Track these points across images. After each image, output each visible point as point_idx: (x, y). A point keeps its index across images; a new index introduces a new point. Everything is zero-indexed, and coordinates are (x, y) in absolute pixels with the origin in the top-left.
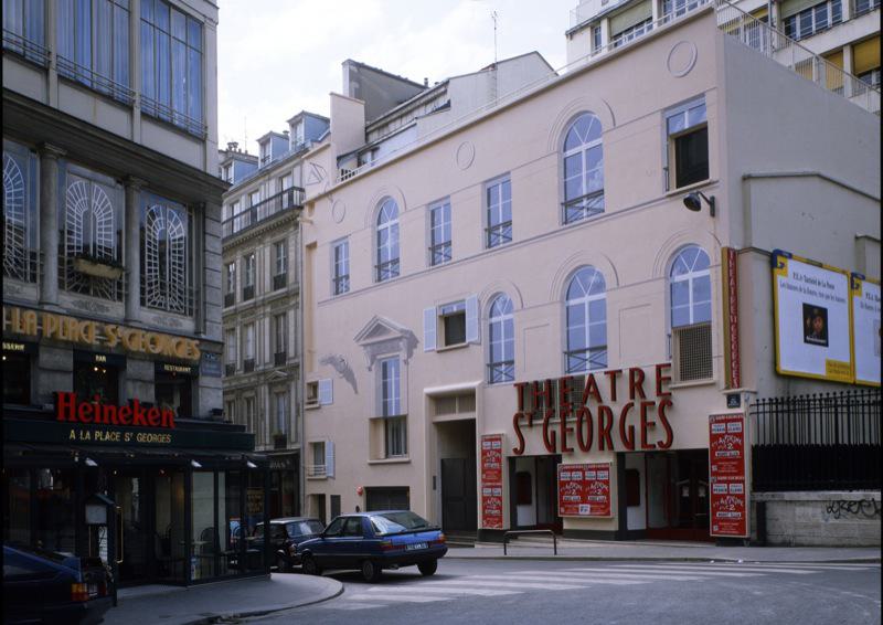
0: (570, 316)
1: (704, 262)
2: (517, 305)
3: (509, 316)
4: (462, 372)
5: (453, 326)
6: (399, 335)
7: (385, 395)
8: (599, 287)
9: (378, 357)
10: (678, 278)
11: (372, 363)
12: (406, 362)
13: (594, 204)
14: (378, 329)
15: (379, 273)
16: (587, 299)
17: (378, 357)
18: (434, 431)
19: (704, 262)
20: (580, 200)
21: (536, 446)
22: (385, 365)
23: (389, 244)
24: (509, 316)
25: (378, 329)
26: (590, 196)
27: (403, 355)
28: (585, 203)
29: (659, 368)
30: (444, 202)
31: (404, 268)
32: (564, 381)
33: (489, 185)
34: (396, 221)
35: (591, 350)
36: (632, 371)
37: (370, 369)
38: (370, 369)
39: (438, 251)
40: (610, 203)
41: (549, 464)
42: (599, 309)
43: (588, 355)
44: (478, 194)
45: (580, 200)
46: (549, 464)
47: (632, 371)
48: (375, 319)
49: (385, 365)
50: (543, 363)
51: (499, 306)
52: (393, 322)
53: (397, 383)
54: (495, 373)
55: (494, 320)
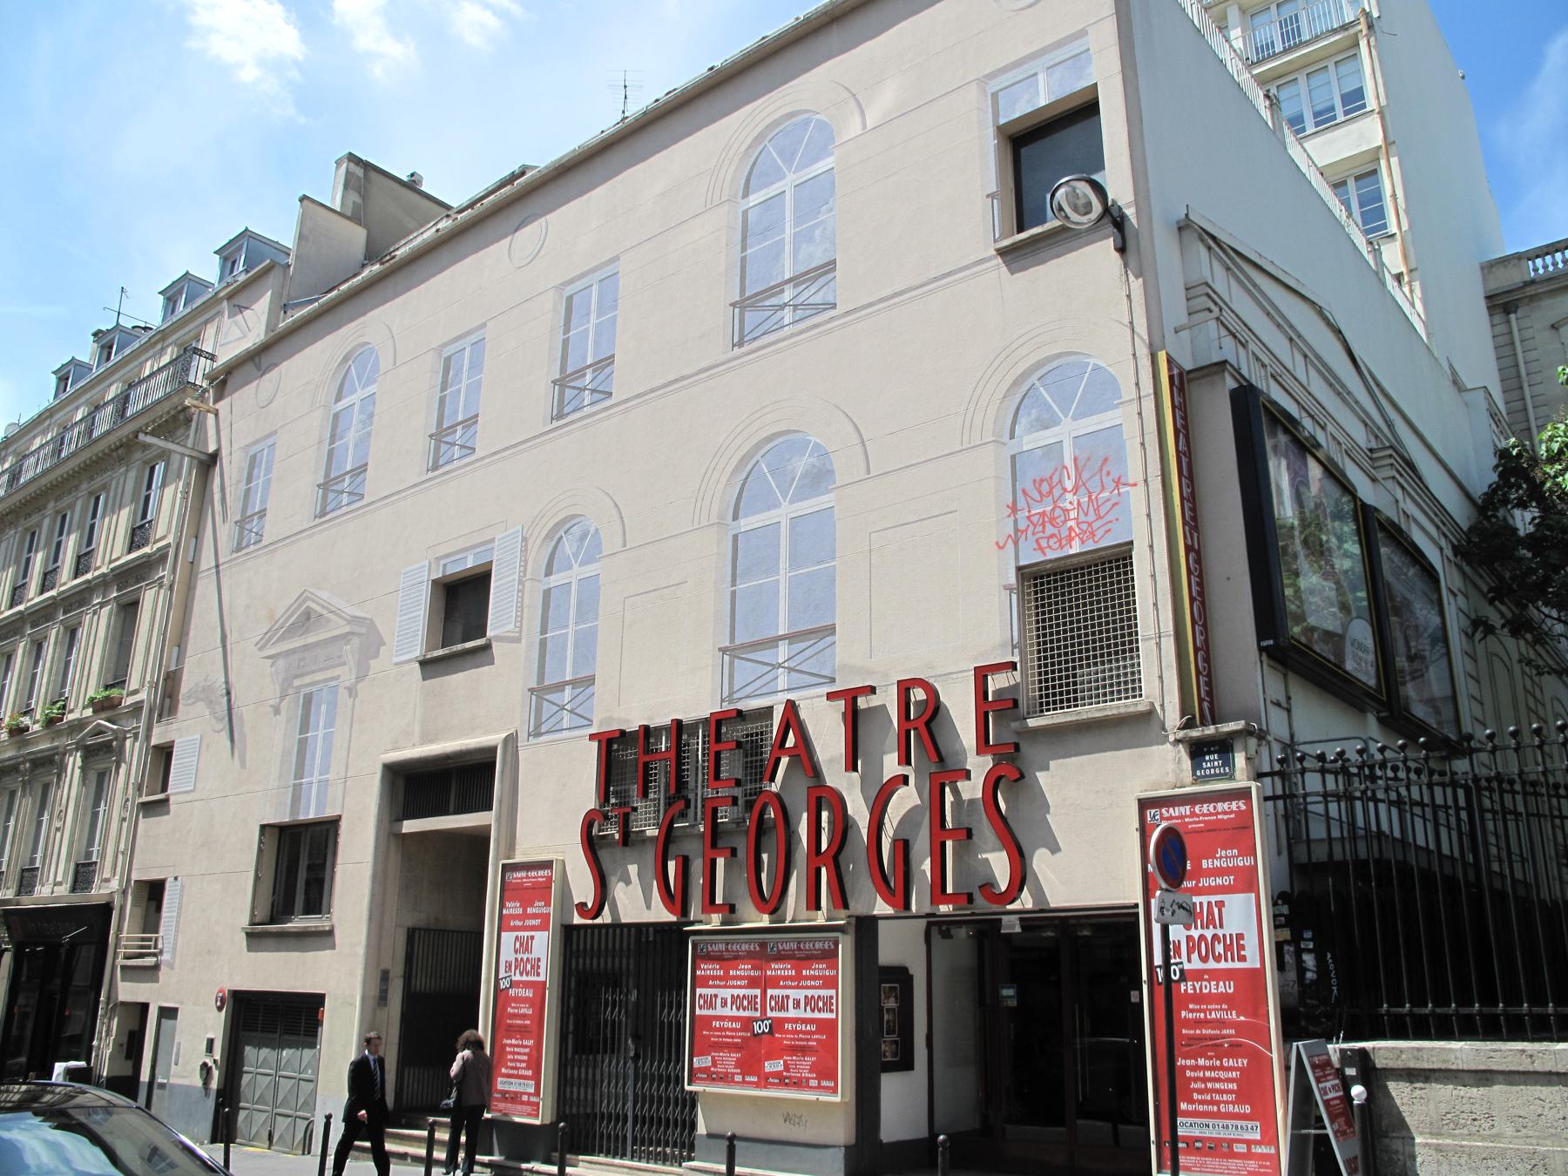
0: (741, 558)
1: (1102, 392)
2: (610, 543)
3: (589, 570)
4: (467, 714)
5: (462, 601)
6: (347, 629)
7: (300, 772)
8: (819, 479)
9: (297, 683)
10: (1030, 440)
11: (283, 697)
12: (352, 691)
13: (812, 294)
14: (307, 619)
15: (325, 497)
16: (784, 512)
17: (297, 683)
18: (395, 859)
19: (1102, 392)
20: (777, 289)
21: (637, 902)
22: (308, 700)
23: (351, 437)
24: (589, 570)
25: (307, 619)
26: (795, 280)
27: (346, 675)
28: (787, 296)
29: (982, 674)
30: (473, 338)
31: (374, 485)
32: (717, 723)
33: (569, 290)
34: (372, 389)
35: (792, 638)
36: (905, 687)
37: (277, 711)
38: (277, 711)
39: (449, 439)
40: (845, 289)
41: (661, 957)
42: (814, 538)
43: (783, 652)
44: (548, 311)
45: (777, 289)
46: (661, 957)
47: (905, 687)
48: (303, 597)
49: (308, 700)
50: (670, 686)
51: (568, 547)
52: (339, 603)
53: (328, 738)
54: (548, 709)
55: (556, 580)
